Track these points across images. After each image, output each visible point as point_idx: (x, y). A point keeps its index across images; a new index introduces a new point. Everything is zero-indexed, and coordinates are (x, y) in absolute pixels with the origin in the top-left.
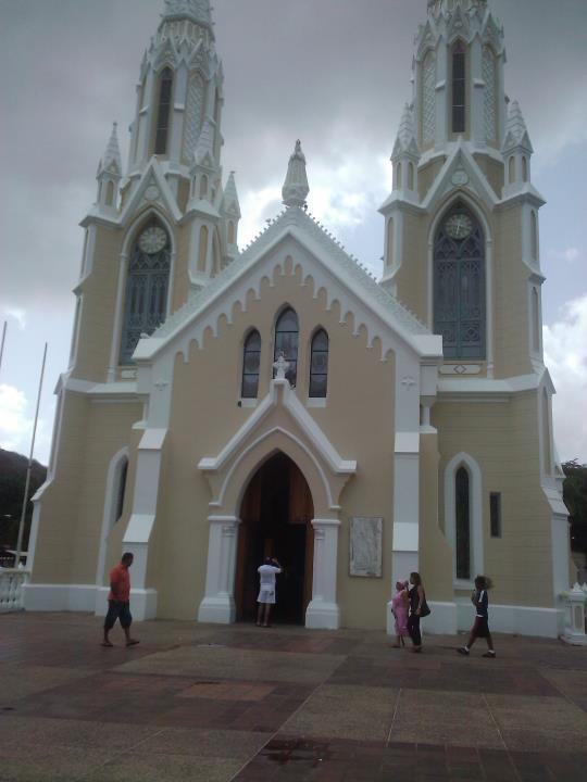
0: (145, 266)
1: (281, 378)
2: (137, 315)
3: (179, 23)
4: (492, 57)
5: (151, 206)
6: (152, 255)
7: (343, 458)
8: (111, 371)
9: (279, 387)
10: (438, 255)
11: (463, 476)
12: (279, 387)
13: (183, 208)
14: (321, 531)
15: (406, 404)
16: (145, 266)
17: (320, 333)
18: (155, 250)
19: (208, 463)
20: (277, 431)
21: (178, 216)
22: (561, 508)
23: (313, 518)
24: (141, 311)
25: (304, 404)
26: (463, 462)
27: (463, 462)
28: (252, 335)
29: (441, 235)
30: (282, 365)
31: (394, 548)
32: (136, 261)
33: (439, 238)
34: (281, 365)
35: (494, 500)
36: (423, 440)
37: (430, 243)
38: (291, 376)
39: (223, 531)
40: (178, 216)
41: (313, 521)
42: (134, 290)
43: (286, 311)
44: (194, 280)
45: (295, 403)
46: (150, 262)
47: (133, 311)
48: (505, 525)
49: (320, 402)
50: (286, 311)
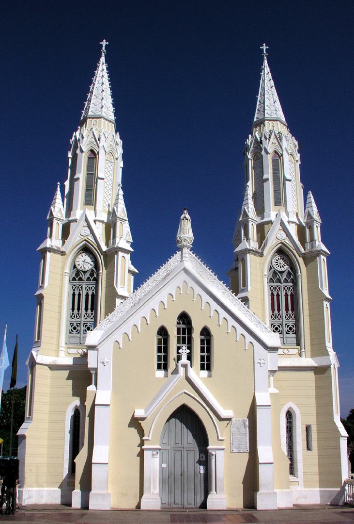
0: (81, 279)
1: (184, 360)
2: (76, 311)
3: (97, 120)
4: (293, 162)
5: (85, 240)
6: (85, 272)
7: (225, 409)
8: (63, 349)
9: (185, 366)
10: (271, 280)
11: (289, 415)
12: (185, 366)
13: (107, 244)
14: (214, 453)
15: (261, 374)
16: (81, 279)
17: (206, 332)
18: (87, 269)
19: (139, 413)
20: (185, 393)
21: (104, 248)
22: (343, 432)
23: (208, 446)
24: (79, 309)
25: (198, 375)
26: (290, 408)
27: (290, 408)
28: (163, 332)
29: (271, 268)
30: (184, 351)
31: (260, 462)
32: (74, 275)
33: (270, 270)
34: (184, 351)
35: (308, 429)
36: (272, 395)
37: (266, 273)
38: (189, 358)
39: (153, 455)
40: (104, 248)
41: (208, 447)
42: (74, 295)
43: (184, 318)
44: (120, 293)
45: (198, 376)
46: (85, 277)
47: (73, 309)
48: (314, 444)
49: (205, 373)
50: (184, 318)
